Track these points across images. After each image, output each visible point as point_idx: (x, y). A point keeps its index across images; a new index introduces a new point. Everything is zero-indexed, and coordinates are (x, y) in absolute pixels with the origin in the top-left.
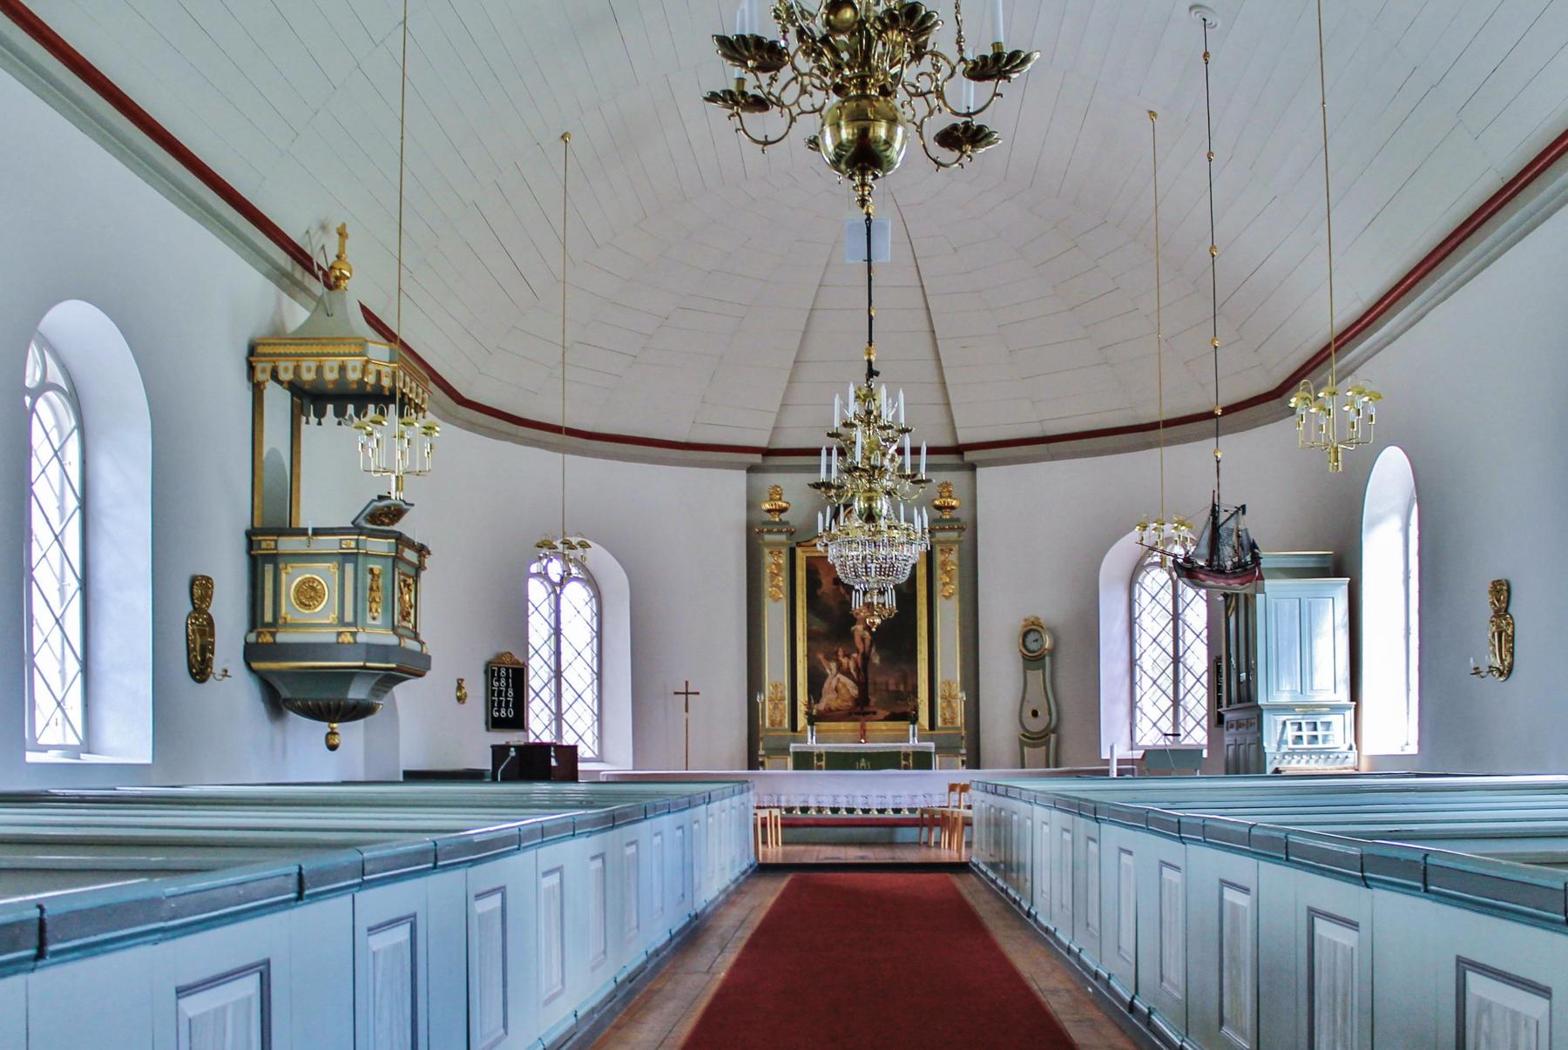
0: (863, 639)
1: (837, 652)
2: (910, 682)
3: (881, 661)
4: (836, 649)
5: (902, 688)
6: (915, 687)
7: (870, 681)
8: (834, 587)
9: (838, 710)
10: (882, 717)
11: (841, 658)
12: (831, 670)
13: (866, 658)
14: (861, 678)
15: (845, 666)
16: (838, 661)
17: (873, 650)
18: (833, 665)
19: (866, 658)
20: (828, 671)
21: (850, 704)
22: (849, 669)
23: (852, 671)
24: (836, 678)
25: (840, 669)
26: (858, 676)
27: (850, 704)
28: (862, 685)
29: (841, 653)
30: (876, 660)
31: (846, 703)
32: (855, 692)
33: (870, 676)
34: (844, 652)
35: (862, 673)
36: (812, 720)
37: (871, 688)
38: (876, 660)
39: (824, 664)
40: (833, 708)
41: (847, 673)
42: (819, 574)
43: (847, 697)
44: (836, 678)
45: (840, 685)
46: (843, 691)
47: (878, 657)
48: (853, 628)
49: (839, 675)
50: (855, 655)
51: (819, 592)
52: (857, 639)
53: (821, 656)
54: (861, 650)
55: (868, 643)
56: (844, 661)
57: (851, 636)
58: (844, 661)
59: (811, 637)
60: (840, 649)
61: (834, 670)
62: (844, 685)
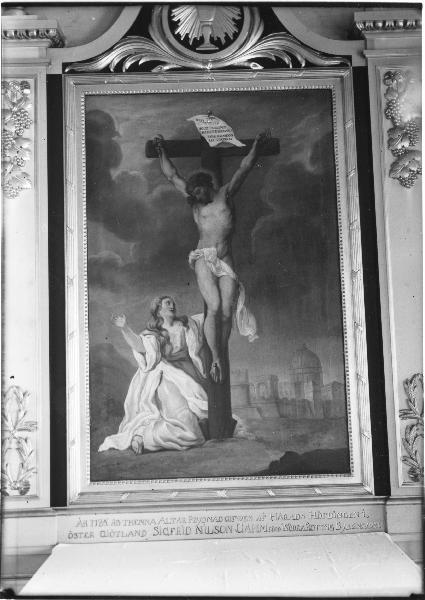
0: (217, 281)
1: (155, 314)
2: (328, 379)
3: (259, 332)
4: (154, 306)
5: (309, 395)
6: (342, 387)
7: (233, 380)
8: (149, 161)
9: (163, 450)
10: (265, 465)
11: (166, 325)
12: (143, 354)
13: (223, 324)
14: (213, 370)
15: (177, 343)
16: (158, 330)
17: (240, 306)
18: (149, 342)
19: (223, 324)
20: (138, 357)
21: (190, 434)
22: (184, 348)
23: (192, 354)
24: (155, 373)
25: (165, 353)
26: (207, 368)
27: (190, 434)
28: (217, 389)
29: (165, 312)
30: (246, 327)
31: (179, 433)
32: (199, 404)
33: (234, 367)
34: (173, 311)
35: (216, 361)
36: (104, 469)
37: (236, 398)
38: (246, 327)
39: (130, 342)
40: (149, 446)
41: (180, 360)
42: (117, 134)
43: (181, 416)
44: (155, 373)
45: (164, 390)
46: (171, 403)
47: (252, 321)
48: (192, 255)
49: (164, 366)
50: (199, 317)
51: (115, 173)
52: (203, 273)
53: (121, 322)
54: (213, 305)
55: (227, 287)
56: (175, 331)
57: (188, 276)
58: (175, 331)
59: (97, 274)
60: (164, 304)
61: (152, 353)
62: (176, 391)
